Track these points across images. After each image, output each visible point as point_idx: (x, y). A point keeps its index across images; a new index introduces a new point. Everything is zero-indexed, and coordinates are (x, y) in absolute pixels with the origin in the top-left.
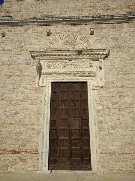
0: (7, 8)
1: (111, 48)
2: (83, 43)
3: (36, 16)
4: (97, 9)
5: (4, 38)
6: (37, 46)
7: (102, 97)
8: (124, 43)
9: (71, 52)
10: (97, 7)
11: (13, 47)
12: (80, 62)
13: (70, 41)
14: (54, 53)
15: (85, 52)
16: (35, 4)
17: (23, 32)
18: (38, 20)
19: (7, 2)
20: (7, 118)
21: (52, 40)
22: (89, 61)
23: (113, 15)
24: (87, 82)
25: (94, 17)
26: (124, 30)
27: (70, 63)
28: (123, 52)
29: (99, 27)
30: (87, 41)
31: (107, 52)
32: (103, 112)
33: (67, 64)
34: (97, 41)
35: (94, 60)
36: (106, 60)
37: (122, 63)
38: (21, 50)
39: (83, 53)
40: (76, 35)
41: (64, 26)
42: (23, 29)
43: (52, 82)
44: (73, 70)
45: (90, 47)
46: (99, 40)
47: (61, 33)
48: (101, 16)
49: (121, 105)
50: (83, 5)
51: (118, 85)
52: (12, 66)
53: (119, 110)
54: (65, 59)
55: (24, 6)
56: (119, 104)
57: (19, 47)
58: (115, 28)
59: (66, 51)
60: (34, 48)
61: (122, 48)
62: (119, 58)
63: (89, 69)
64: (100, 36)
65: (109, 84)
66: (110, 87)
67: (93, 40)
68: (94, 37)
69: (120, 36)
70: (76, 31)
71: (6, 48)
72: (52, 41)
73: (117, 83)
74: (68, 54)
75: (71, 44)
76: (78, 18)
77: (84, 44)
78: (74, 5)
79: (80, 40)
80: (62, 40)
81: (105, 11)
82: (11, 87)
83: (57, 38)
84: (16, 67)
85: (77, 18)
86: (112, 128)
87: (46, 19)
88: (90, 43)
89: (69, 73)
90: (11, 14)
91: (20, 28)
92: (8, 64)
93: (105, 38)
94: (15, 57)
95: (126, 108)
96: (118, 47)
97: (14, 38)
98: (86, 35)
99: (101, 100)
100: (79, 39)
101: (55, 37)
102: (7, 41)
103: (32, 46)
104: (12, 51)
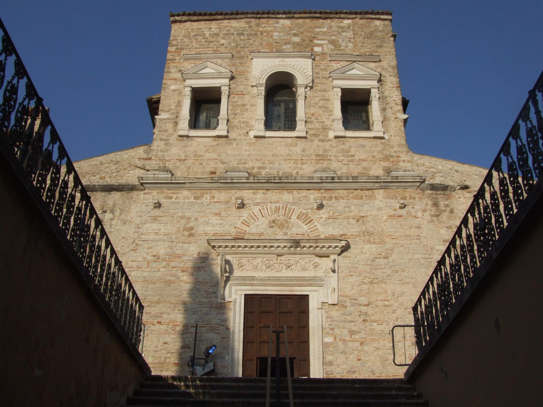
0: (160, 151)
1: (352, 235)
2: (303, 225)
3: (216, 169)
4: (330, 160)
5: (157, 212)
6: (218, 229)
7: (333, 323)
8: (376, 227)
9: (281, 243)
10: (331, 156)
11: (174, 228)
12: (298, 259)
13: (279, 220)
14: (250, 243)
15: (305, 242)
16: (214, 146)
17: (192, 200)
18: (220, 180)
19: (161, 140)
20: (169, 355)
21: (247, 218)
22: (312, 259)
23: (356, 177)
24: (308, 295)
25: (323, 178)
26: (377, 202)
27: (278, 261)
28: (374, 243)
29: (333, 196)
30: (309, 222)
31: (343, 243)
32: (333, 347)
34: (327, 222)
35: (321, 257)
36: (343, 257)
37: (369, 262)
38: (191, 235)
39: (302, 245)
40: (290, 209)
41: (269, 192)
42: (192, 194)
43: (245, 295)
44: (285, 273)
45: (314, 234)
46: (331, 221)
47: (264, 204)
48: (336, 178)
49: (364, 336)
50: (304, 150)
51: (361, 303)
52: (173, 264)
53: (362, 344)
54: (270, 253)
55: (192, 149)
56: (362, 335)
57: (185, 229)
58: (362, 198)
59: (273, 241)
60: (214, 232)
61: (372, 235)
62: (365, 253)
63: (310, 274)
64: (334, 213)
65: (345, 299)
66: (348, 304)
67: (321, 221)
68: (323, 214)
69: (369, 213)
70: (291, 200)
71: (162, 230)
72: (247, 220)
73: (360, 299)
74: (276, 245)
75: (281, 226)
76: (295, 180)
78: (287, 151)
79: (297, 218)
80: (264, 218)
81: (345, 164)
82: (173, 301)
84: (182, 265)
85: (292, 179)
86: (347, 373)
87: (235, 178)
90: (169, 164)
91: (185, 193)
92: (167, 260)
94: (177, 248)
95: (373, 340)
96: (366, 234)
97: (176, 211)
98: (309, 211)
99: (330, 327)
100: (296, 218)
102: (162, 217)
103: (209, 229)
104: (174, 236)
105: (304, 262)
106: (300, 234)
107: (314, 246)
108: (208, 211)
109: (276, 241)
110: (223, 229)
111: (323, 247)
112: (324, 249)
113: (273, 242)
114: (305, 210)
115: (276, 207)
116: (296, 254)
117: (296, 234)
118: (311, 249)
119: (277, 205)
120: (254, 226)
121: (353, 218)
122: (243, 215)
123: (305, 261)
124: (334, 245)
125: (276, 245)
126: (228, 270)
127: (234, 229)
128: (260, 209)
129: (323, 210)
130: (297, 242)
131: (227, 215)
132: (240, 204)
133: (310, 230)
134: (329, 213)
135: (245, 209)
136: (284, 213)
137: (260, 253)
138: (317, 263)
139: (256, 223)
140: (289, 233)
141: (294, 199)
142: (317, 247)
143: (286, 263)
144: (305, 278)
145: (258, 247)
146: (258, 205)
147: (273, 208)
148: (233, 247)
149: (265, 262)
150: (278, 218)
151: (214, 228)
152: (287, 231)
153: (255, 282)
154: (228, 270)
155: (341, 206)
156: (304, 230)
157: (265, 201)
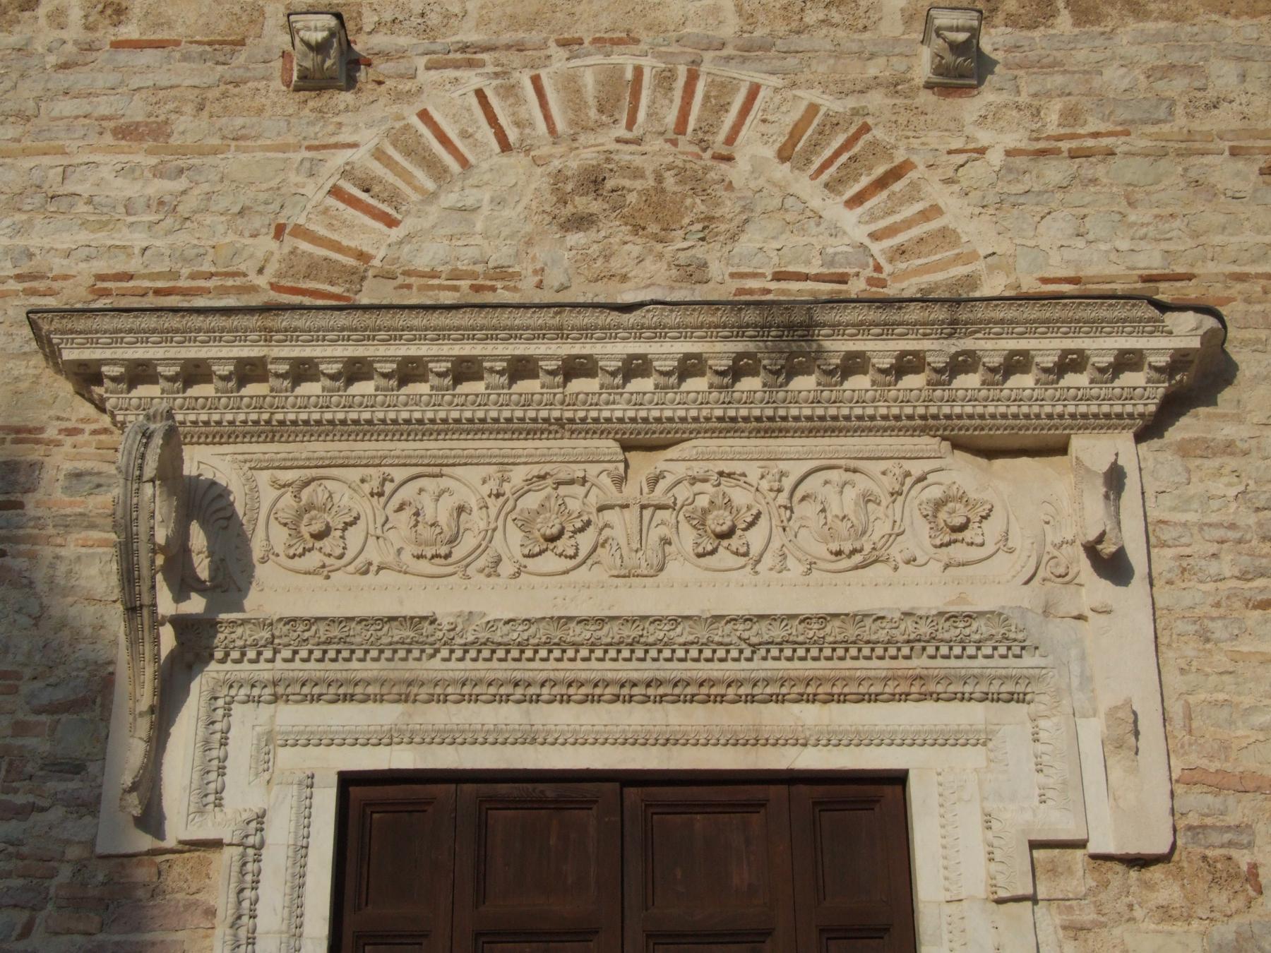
1: (1241, 278)
2: (834, 208)
9: (659, 332)
13: (638, 174)
21: (379, 154)
22: (917, 468)
24: (898, 779)
27: (631, 491)
30: (881, 183)
33: (594, 499)
34: (1027, 182)
35: (990, 452)
36: (1184, 450)
39: (838, 347)
40: (723, 89)
43: (348, 781)
45: (926, 269)
46: (1055, 171)
47: (515, 59)
59: (587, 318)
60: (101, 266)
64: (1071, 115)
67: (977, 172)
72: (378, 169)
74: (612, 351)
77: (849, 219)
79: (784, 155)
80: (517, 162)
83: (452, 134)
88: (934, 211)
89: (610, 632)
93: (1144, 143)
100: (769, 152)
101: (424, 116)
105: (850, 494)
106: (813, 270)
107: (939, 361)
108: (66, 107)
109: (615, 317)
110: (181, 238)
111: (1016, 363)
112: (1023, 381)
113: (586, 332)
114: (843, 94)
115: (619, 69)
116: (783, 432)
117: (778, 277)
118: (913, 381)
119: (615, 59)
120: (433, 211)
121: (1235, 152)
122: (345, 137)
123: (862, 483)
124: (1103, 347)
125: (612, 351)
126: (203, 569)
127: (267, 243)
128: (480, 94)
129: (988, 96)
130: (791, 327)
131: (216, 141)
132: (320, 48)
133: (887, 243)
134: (1037, 113)
135: (365, 97)
136: (671, 117)
137: (478, 427)
138: (962, 498)
139: (450, 199)
140: (716, 269)
141: (750, 19)
142: (961, 364)
143: (703, 502)
144: (870, 630)
145: (465, 370)
146: (471, 64)
147: (589, 81)
148: (249, 371)
149: (520, 494)
150: (626, 155)
151: (103, 238)
152: (700, 252)
153: (435, 667)
154: (203, 569)
155: (1129, 64)
156: (838, 246)
157: (521, 35)
